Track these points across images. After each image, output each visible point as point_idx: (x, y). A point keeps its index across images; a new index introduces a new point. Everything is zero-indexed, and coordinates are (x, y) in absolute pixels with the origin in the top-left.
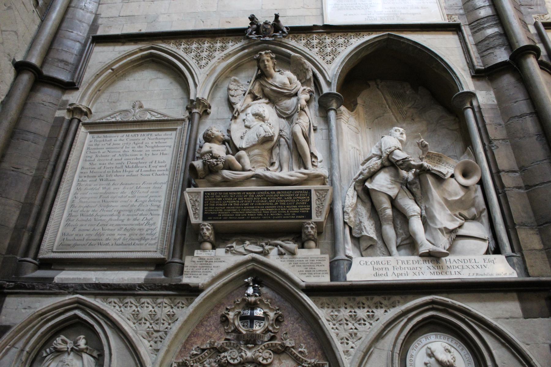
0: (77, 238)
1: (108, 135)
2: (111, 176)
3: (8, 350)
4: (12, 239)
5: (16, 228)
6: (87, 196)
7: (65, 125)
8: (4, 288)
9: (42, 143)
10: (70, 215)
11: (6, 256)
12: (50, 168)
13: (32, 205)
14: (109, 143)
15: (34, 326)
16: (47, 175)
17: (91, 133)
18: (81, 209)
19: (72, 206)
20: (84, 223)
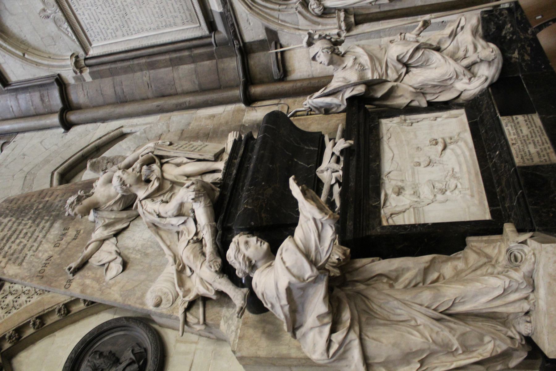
0: (182, 11)
1: (85, 29)
2: (119, 7)
3: (282, 21)
4: (203, 60)
5: (193, 62)
6: (145, 19)
7: (95, 69)
8: (240, 47)
9: (118, 79)
10: (166, 26)
11: (217, 58)
12: (136, 62)
13: (171, 60)
14: (91, 24)
15: (260, 10)
16: (143, 61)
17: (91, 45)
18: (157, 19)
19: (158, 28)
20: (168, 11)
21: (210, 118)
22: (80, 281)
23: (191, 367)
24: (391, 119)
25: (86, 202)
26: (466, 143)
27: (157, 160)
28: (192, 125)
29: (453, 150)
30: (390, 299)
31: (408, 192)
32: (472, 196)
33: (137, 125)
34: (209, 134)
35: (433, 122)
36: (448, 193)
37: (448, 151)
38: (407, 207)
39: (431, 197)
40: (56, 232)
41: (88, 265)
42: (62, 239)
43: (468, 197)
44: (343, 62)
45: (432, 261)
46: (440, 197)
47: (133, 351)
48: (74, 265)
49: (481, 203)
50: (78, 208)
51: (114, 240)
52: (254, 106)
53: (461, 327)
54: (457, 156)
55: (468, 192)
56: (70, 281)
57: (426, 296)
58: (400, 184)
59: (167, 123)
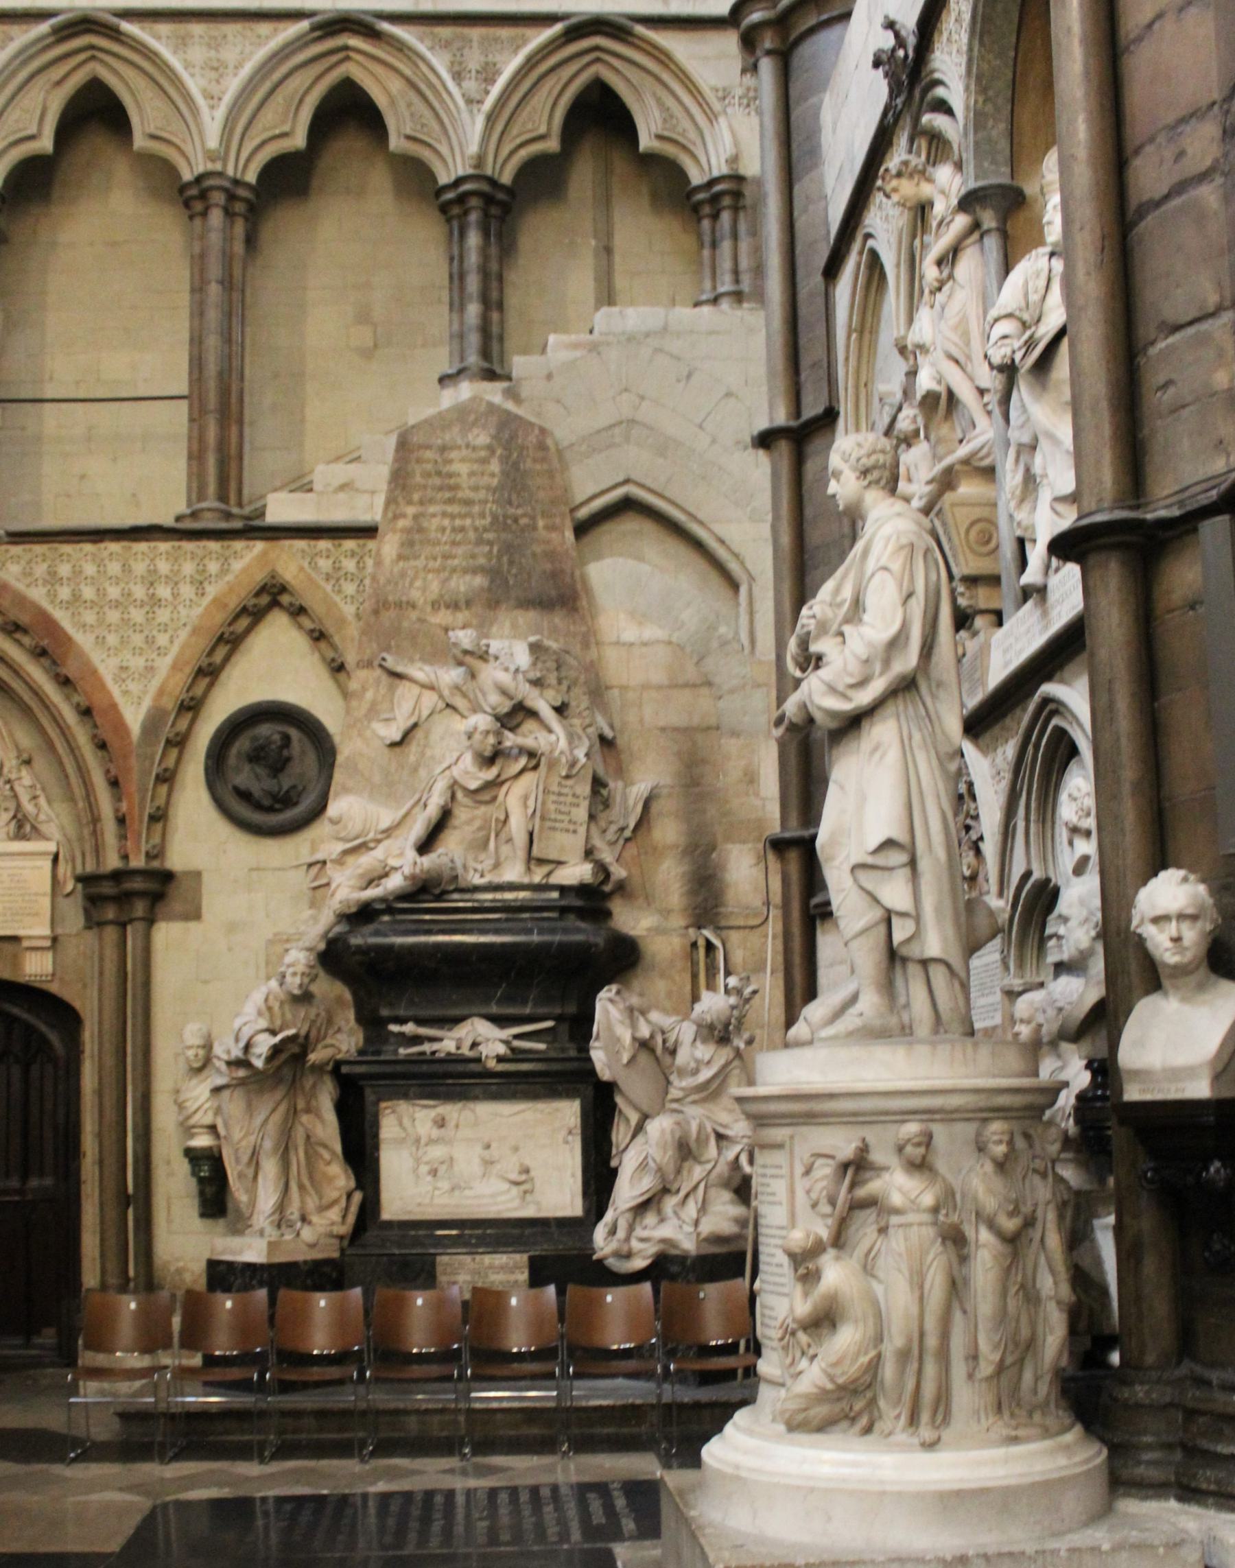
21: (746, 775)
22: (371, 681)
23: (279, 869)
24: (579, 1113)
25: (468, 659)
26: (516, 1209)
27: (533, 762)
28: (733, 741)
29: (508, 1191)
30: (267, 1113)
31: (435, 1133)
32: (419, 1205)
33: (751, 613)
34: (698, 785)
35: (569, 1173)
36: (429, 1178)
37: (506, 1186)
38: (410, 1130)
39: (425, 1159)
40: (462, 589)
41: (397, 681)
42: (448, 607)
43: (419, 1200)
44: (704, 1041)
45: (333, 1153)
46: (424, 1169)
47: (294, 787)
48: (391, 662)
49: (410, 1212)
50: (457, 652)
51: (441, 705)
52: (771, 857)
53: (250, 1172)
54: (493, 1196)
55: (427, 1201)
56: (369, 664)
57: (268, 1144)
58: (453, 1123)
59: (744, 687)
